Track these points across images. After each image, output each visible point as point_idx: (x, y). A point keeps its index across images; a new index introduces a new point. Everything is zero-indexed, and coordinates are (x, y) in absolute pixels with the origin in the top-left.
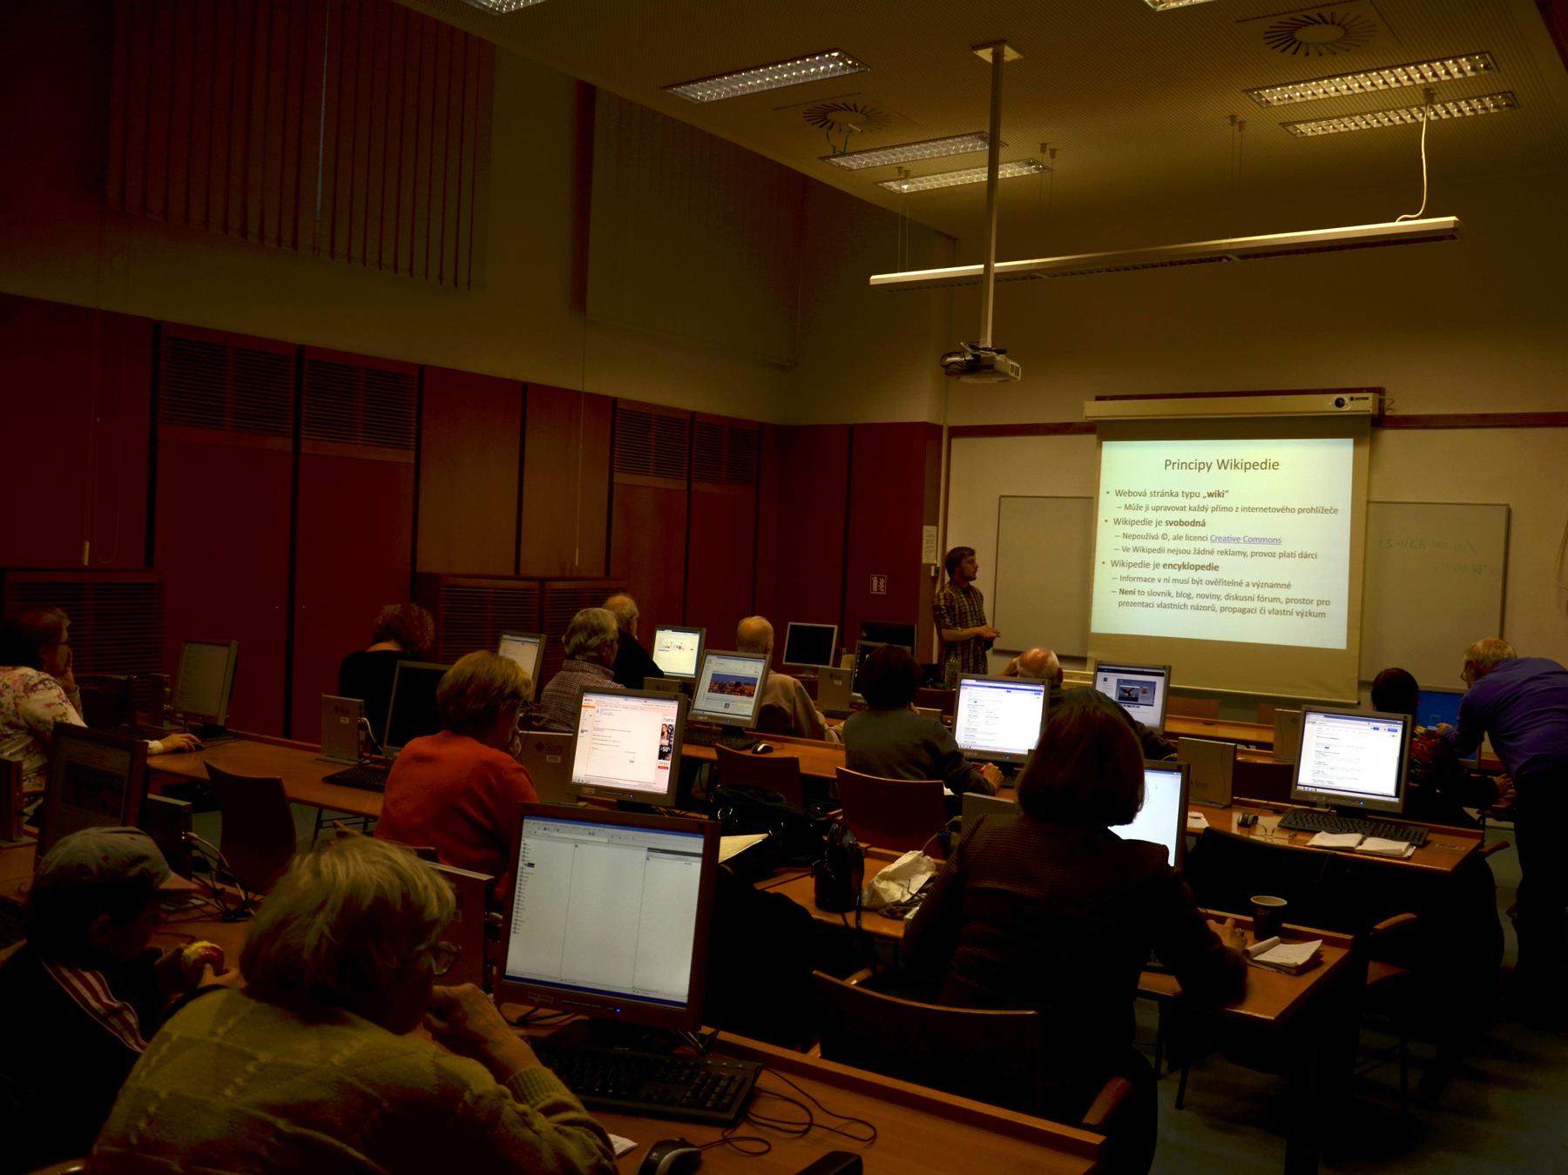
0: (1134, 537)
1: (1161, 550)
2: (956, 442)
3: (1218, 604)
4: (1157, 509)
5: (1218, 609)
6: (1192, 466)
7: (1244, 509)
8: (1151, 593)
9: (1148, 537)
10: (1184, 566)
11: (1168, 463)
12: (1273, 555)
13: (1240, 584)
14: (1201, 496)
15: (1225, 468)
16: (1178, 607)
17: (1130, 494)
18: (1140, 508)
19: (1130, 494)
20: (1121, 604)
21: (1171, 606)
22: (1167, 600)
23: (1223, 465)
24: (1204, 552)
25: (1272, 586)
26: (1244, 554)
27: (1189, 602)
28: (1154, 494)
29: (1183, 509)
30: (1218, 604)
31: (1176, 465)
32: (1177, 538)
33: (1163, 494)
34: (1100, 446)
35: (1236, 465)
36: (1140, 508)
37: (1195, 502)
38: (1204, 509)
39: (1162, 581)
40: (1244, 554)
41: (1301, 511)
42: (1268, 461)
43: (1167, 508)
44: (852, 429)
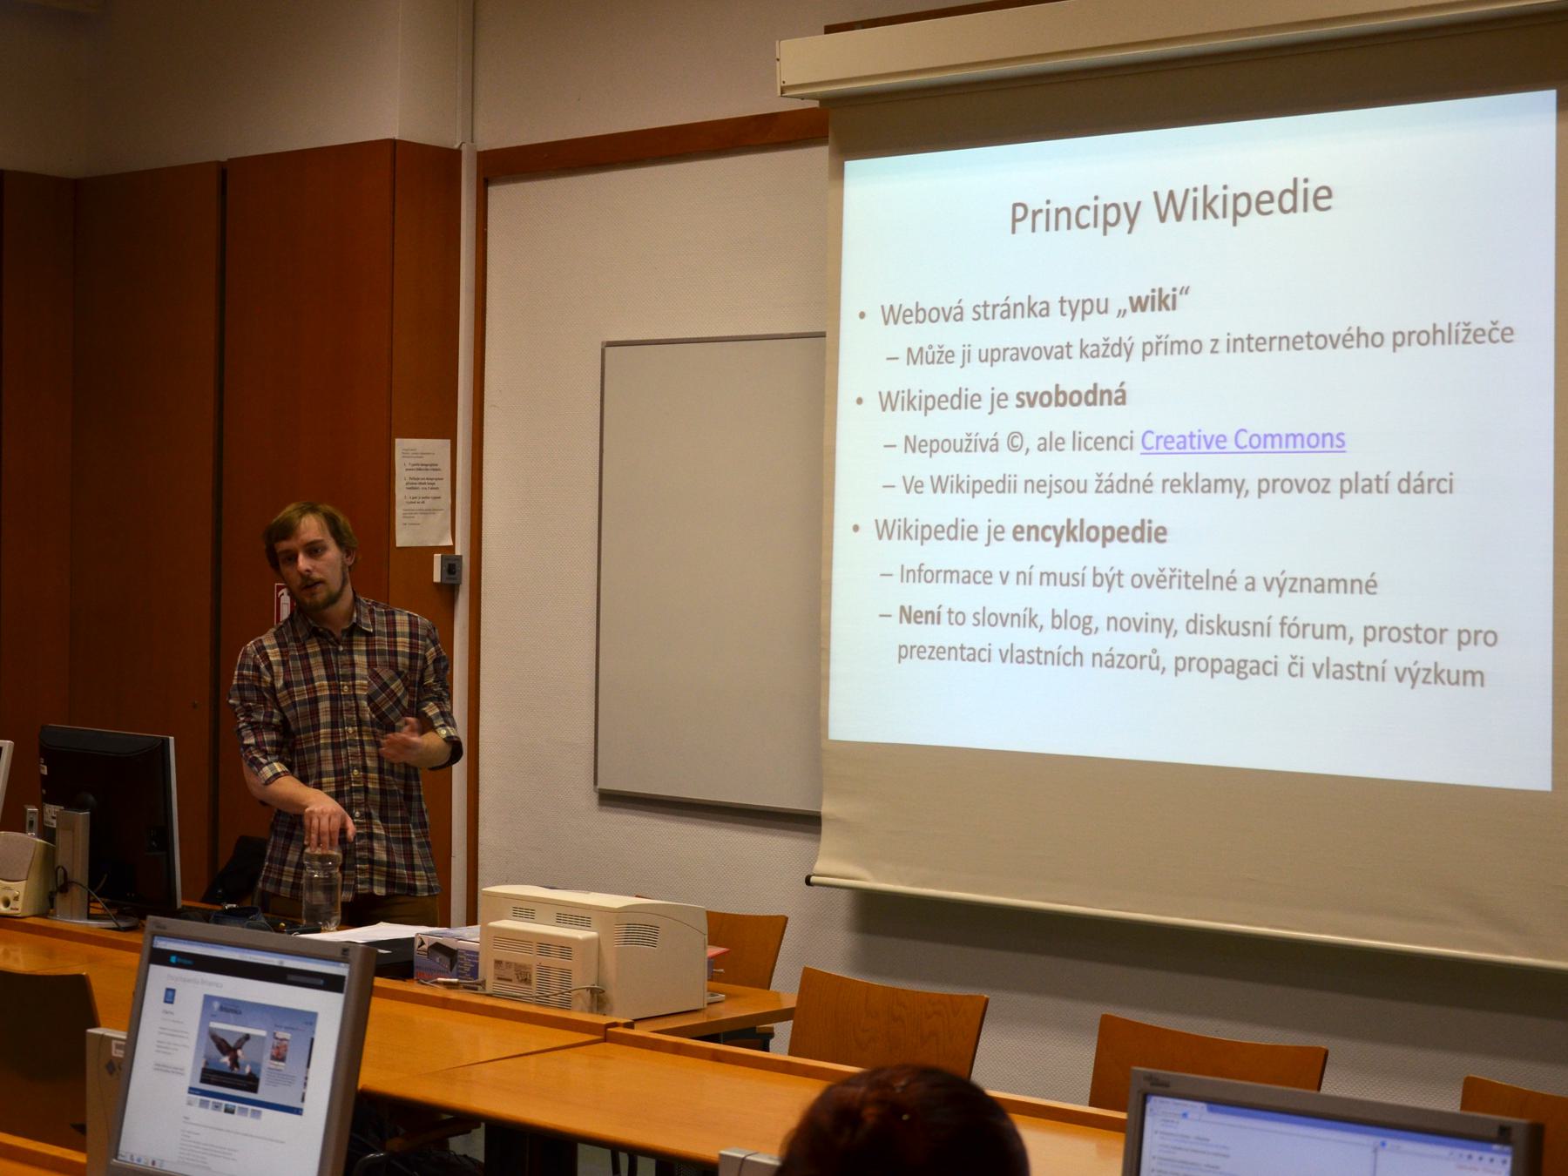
0: (934, 447)
1: (1005, 485)
2: (500, 195)
3: (1169, 649)
4: (992, 356)
5: (1168, 662)
6: (1087, 217)
7: (1234, 344)
8: (986, 619)
9: (972, 444)
10: (1068, 532)
11: (1020, 212)
12: (1322, 487)
13: (1229, 583)
14: (1113, 310)
15: (1179, 217)
16: (1058, 658)
17: (920, 314)
18: (946, 356)
19: (920, 314)
20: (905, 652)
21: (1037, 656)
22: (1026, 639)
23: (1170, 207)
24: (1125, 485)
25: (1322, 587)
26: (1239, 488)
27: (1088, 645)
28: (984, 311)
29: (1063, 352)
30: (1169, 649)
31: (1041, 218)
32: (1050, 444)
33: (1009, 311)
34: (838, 174)
35: (1208, 206)
36: (946, 356)
37: (1095, 329)
38: (1122, 349)
39: (1012, 578)
40: (1239, 488)
41: (1402, 339)
42: (1301, 186)
43: (1020, 354)
44: (224, 172)
